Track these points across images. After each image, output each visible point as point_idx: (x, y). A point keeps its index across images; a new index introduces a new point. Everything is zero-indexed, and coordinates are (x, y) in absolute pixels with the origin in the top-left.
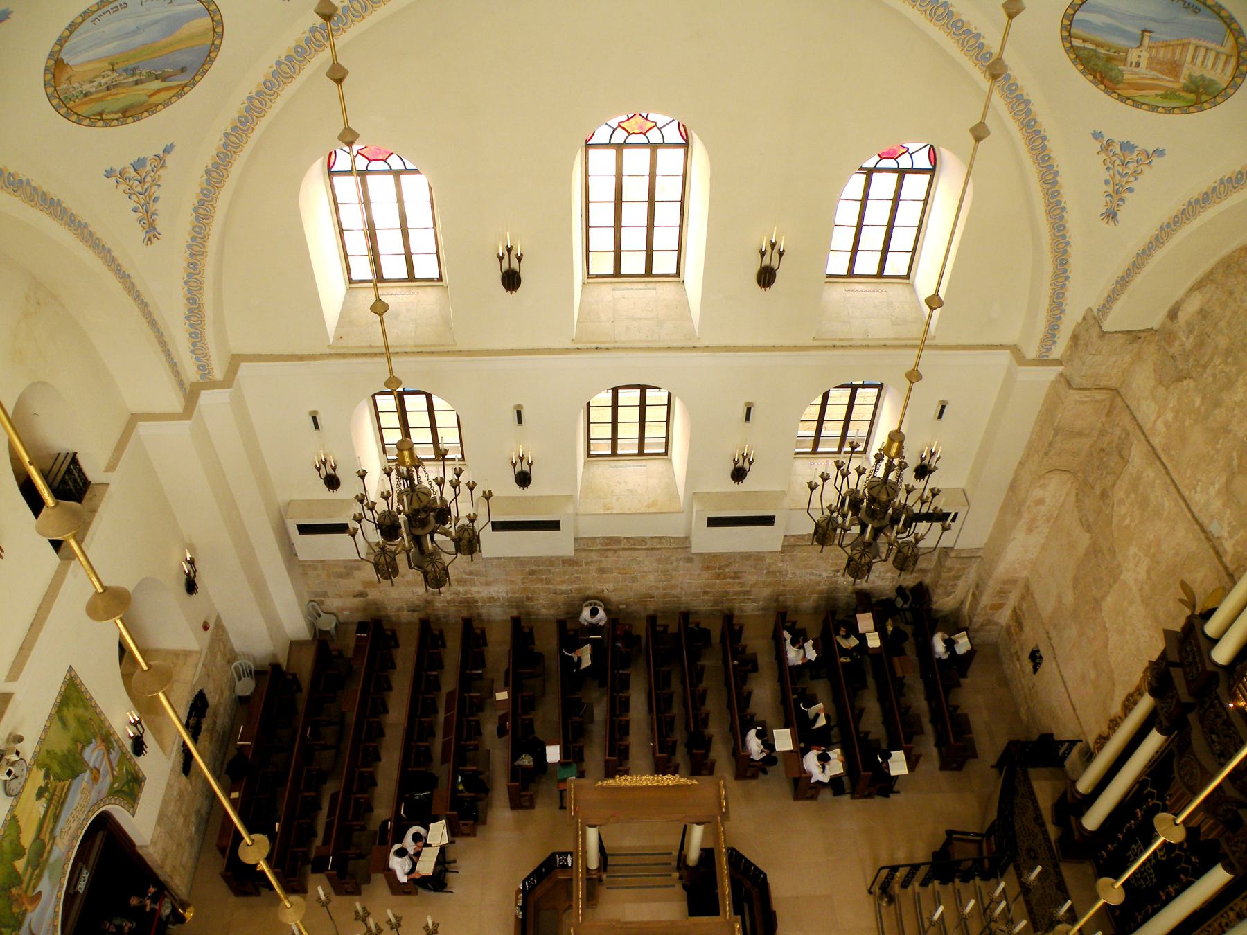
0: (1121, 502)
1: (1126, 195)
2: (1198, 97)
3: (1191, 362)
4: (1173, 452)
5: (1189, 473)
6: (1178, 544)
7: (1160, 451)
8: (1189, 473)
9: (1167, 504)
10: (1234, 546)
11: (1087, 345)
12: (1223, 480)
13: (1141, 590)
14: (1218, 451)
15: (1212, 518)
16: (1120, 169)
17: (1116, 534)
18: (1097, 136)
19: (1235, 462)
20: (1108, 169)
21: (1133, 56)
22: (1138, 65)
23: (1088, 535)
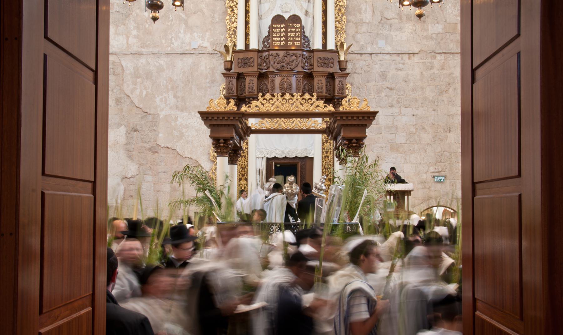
0: (133, 91)
4: (148, 43)
5: (164, 41)
6: (182, 69)
8: (164, 41)
9: (162, 62)
10: (208, 42)
12: (184, 26)
13: (177, 107)
14: (172, 21)
15: (190, 43)
17: (141, 106)
19: (184, 16)
23: (123, 127)
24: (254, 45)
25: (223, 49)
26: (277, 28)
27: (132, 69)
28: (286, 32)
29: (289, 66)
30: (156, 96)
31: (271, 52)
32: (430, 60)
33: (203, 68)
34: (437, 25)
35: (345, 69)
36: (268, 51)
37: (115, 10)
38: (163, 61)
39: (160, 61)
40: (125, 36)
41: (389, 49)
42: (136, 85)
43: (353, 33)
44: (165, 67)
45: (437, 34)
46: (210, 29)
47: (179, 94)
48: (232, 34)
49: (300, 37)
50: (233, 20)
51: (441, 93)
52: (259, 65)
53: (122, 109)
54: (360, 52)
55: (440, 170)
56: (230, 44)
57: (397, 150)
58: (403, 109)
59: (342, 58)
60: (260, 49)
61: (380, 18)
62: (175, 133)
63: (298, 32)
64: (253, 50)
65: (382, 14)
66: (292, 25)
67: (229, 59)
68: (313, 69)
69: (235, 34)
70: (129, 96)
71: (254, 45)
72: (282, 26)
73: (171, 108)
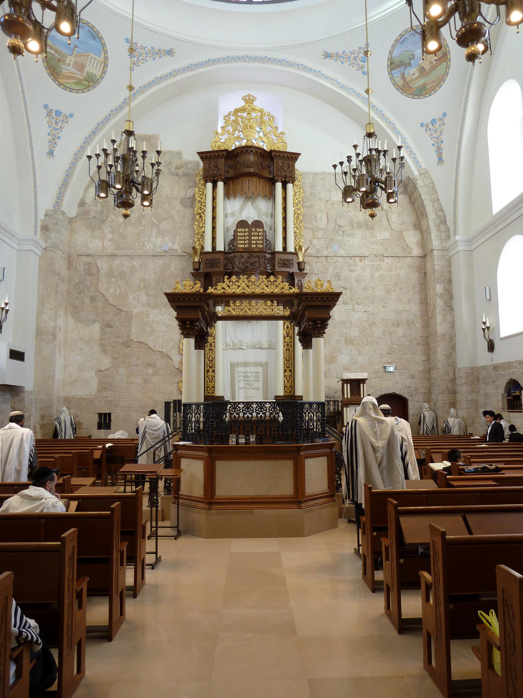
1: (57, 141)
2: (89, 84)
3: (105, 212)
5: (137, 244)
6: (153, 270)
7: (114, 252)
9: (135, 263)
11: (56, 224)
13: (149, 305)
14: (144, 226)
16: (54, 126)
17: (115, 304)
18: (46, 106)
19: (155, 222)
20: (49, 126)
21: (68, 61)
22: (69, 66)
23: (97, 323)
24: (220, 247)
25: (191, 251)
26: (241, 232)
27: (107, 270)
28: (250, 236)
29: (252, 267)
30: (129, 294)
31: (236, 254)
32: (378, 263)
33: (173, 269)
34: (384, 232)
35: (304, 269)
36: (233, 252)
37: (92, 215)
38: (136, 263)
39: (133, 263)
40: (100, 239)
41: (342, 252)
42: (110, 284)
43: (311, 238)
44: (138, 267)
45: (385, 240)
46: (180, 233)
47: (151, 293)
48: (200, 238)
49: (263, 240)
50: (201, 225)
51: (388, 292)
52: (225, 265)
53: (97, 307)
54: (317, 255)
55: (390, 361)
56: (198, 247)
57: (352, 344)
58: (356, 306)
59: (301, 260)
60: (227, 251)
61: (334, 225)
62: (147, 328)
63: (260, 236)
64: (220, 252)
65: (336, 221)
66: (256, 230)
67: (196, 260)
68: (274, 269)
69: (203, 238)
70: (103, 294)
71: (220, 247)
72: (246, 230)
73: (143, 305)
